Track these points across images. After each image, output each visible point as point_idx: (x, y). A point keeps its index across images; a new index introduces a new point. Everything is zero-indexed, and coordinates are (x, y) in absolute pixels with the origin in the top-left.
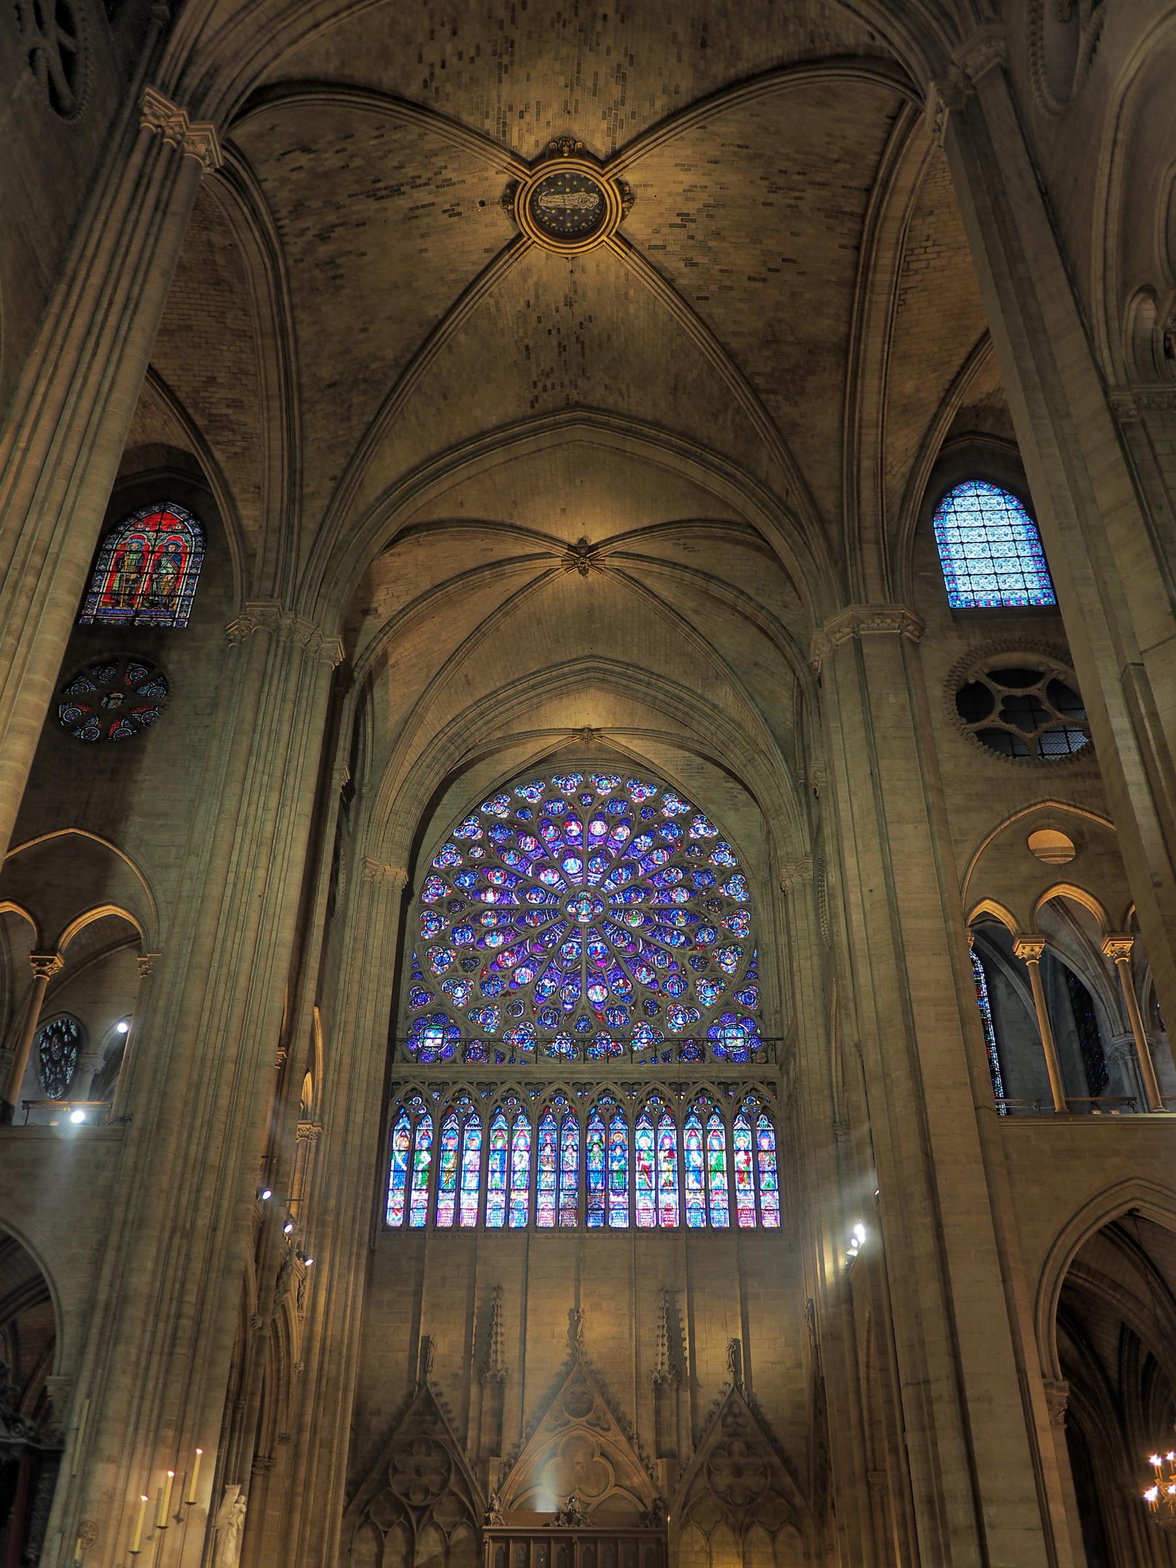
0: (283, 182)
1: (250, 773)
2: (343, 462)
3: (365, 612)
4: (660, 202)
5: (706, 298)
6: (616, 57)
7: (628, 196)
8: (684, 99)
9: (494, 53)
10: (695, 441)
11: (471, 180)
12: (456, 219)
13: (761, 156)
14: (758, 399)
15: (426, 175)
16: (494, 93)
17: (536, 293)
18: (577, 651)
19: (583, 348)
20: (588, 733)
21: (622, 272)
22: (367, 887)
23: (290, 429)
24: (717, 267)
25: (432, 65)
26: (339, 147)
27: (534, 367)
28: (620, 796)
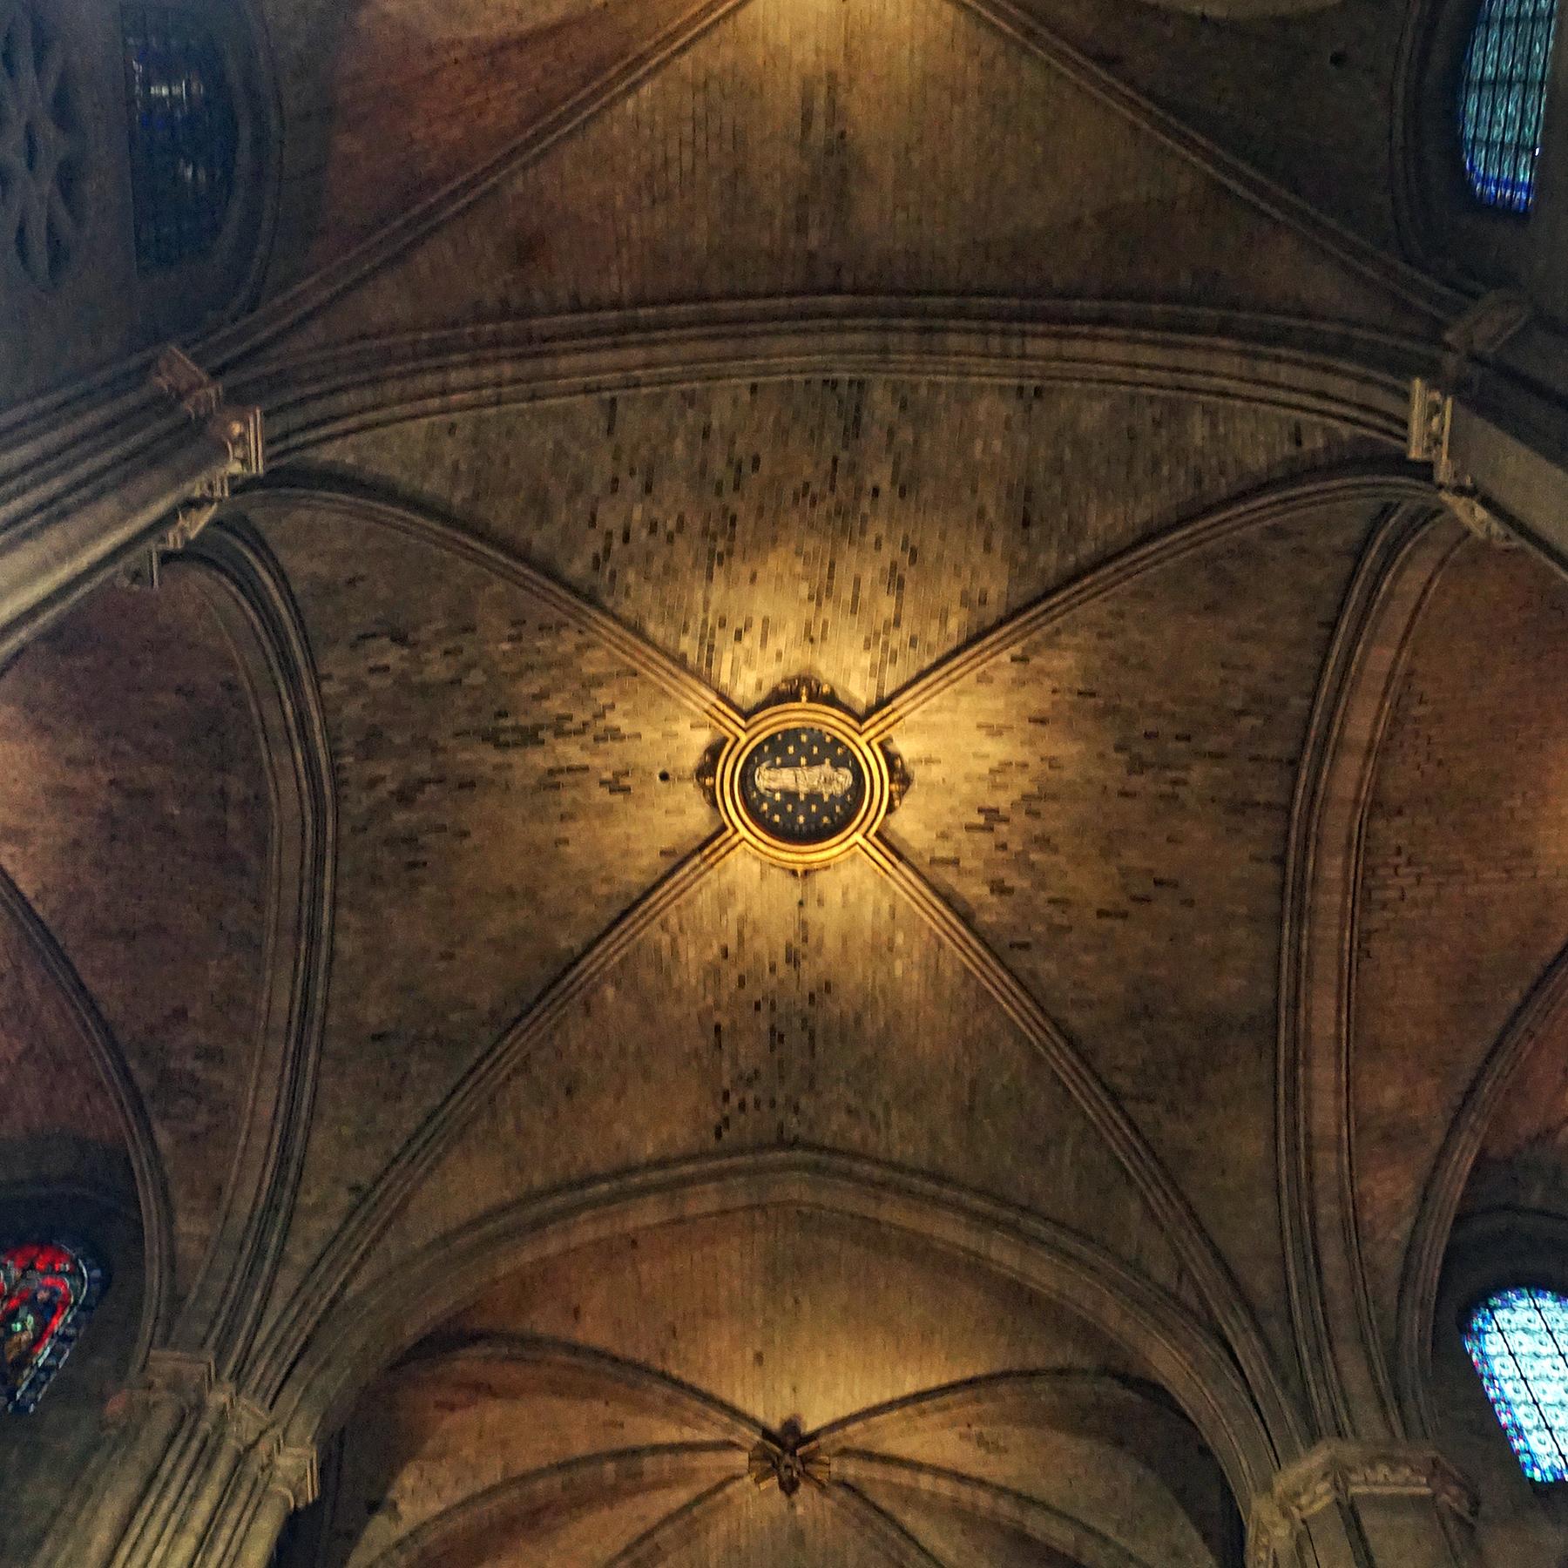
0: (356, 687)
2: (376, 1164)
3: (373, 1507)
4: (950, 791)
5: (1025, 946)
6: (889, 552)
8: (993, 611)
9: (705, 532)
10: (1003, 1202)
11: (649, 734)
12: (619, 797)
13: (1115, 710)
14: (1120, 1108)
15: (581, 716)
16: (699, 595)
17: (740, 934)
19: (812, 1038)
21: (885, 906)
23: (293, 1096)
24: (1044, 895)
25: (609, 534)
26: (451, 645)
27: (726, 1065)
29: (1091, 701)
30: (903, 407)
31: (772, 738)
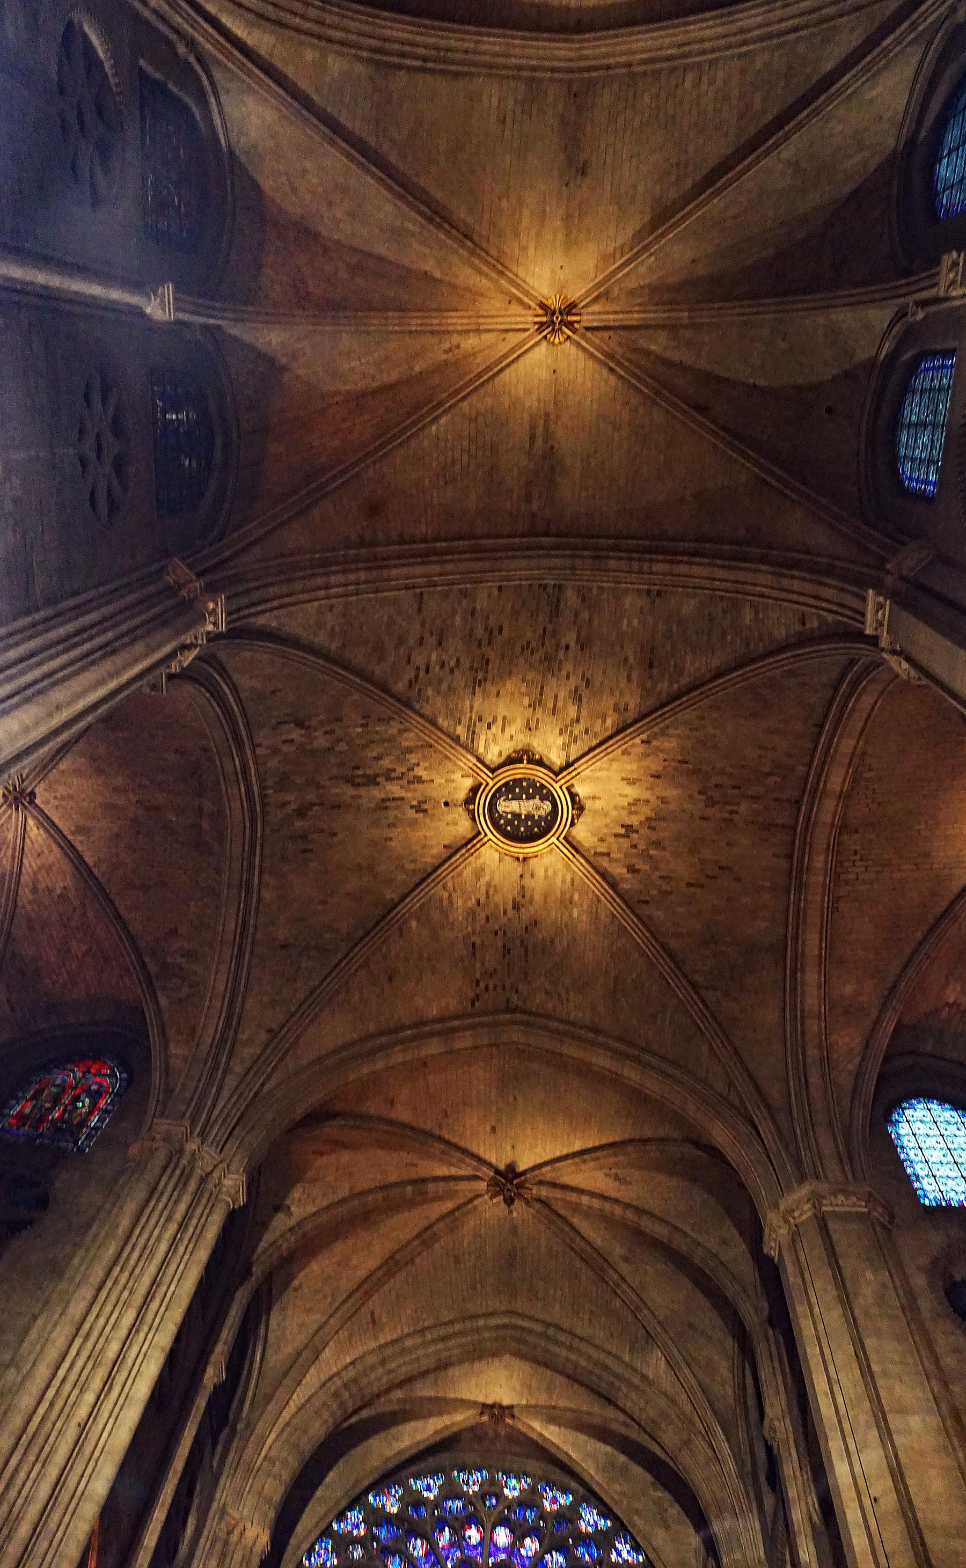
0: (275, 751)
1: (109, 1284)
3: (277, 1209)
5: (646, 902)
6: (574, 681)
7: (578, 806)
8: (631, 715)
9: (471, 668)
10: (631, 1044)
11: (438, 780)
12: (421, 815)
13: (699, 771)
14: (697, 993)
15: (400, 770)
17: (487, 892)
18: (494, 1304)
19: (526, 951)
20: (498, 1411)
21: (569, 878)
22: (218, 1546)
23: (236, 979)
24: (657, 874)
25: (418, 668)
27: (478, 965)
28: (529, 1501)
29: (685, 766)
30: (583, 600)
31: (507, 783)
